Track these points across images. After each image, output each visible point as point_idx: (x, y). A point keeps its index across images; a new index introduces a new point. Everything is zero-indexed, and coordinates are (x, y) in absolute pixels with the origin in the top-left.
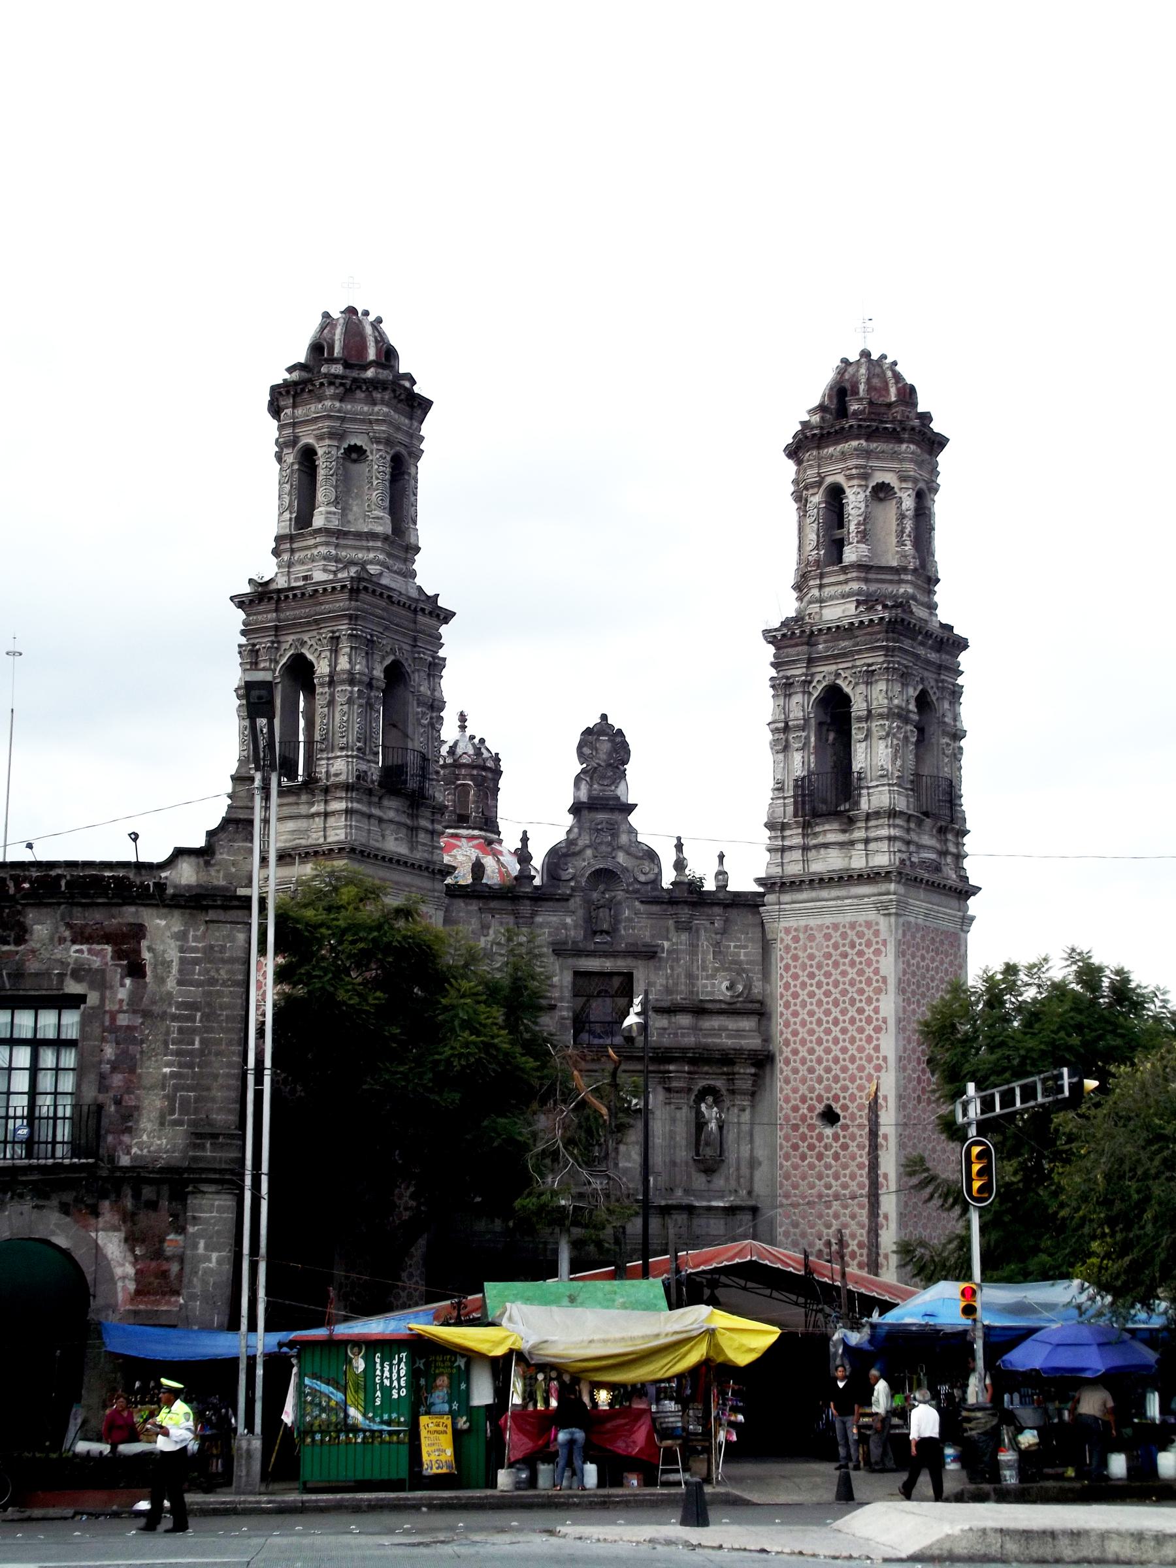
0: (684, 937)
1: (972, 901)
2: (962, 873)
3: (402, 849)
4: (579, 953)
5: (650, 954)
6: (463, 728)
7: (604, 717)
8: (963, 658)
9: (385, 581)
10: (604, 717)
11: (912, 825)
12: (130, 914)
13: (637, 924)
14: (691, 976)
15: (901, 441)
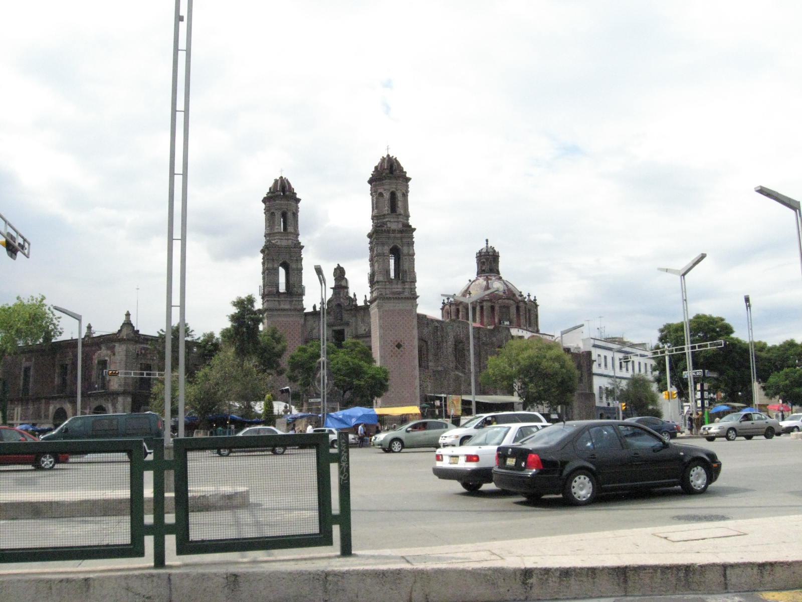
0: (354, 318)
1: (417, 300)
2: (412, 293)
3: (287, 307)
4: (333, 326)
5: (347, 324)
6: (487, 244)
7: (338, 265)
8: (414, 234)
9: (279, 243)
10: (338, 265)
11: (387, 283)
12: (114, 344)
13: (346, 317)
14: (356, 329)
15: (383, 180)
